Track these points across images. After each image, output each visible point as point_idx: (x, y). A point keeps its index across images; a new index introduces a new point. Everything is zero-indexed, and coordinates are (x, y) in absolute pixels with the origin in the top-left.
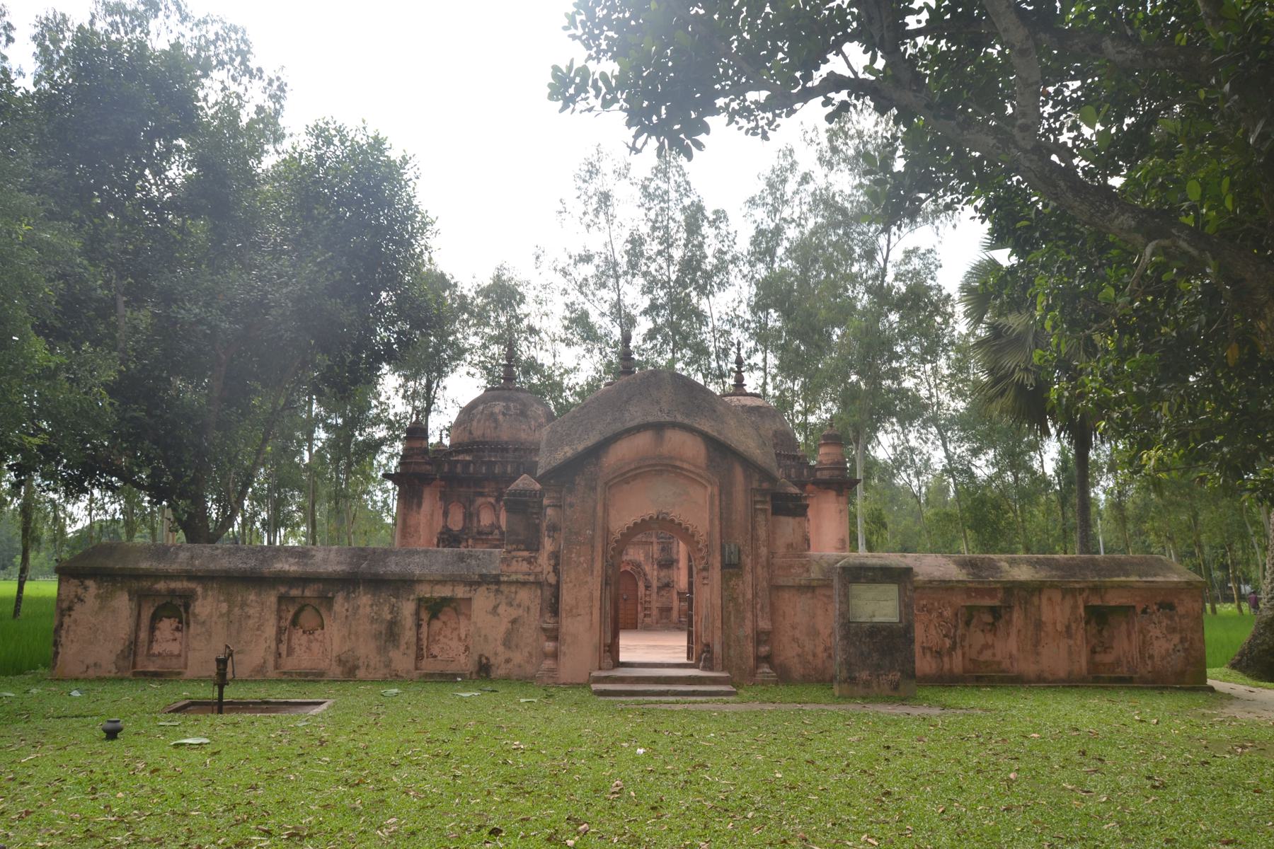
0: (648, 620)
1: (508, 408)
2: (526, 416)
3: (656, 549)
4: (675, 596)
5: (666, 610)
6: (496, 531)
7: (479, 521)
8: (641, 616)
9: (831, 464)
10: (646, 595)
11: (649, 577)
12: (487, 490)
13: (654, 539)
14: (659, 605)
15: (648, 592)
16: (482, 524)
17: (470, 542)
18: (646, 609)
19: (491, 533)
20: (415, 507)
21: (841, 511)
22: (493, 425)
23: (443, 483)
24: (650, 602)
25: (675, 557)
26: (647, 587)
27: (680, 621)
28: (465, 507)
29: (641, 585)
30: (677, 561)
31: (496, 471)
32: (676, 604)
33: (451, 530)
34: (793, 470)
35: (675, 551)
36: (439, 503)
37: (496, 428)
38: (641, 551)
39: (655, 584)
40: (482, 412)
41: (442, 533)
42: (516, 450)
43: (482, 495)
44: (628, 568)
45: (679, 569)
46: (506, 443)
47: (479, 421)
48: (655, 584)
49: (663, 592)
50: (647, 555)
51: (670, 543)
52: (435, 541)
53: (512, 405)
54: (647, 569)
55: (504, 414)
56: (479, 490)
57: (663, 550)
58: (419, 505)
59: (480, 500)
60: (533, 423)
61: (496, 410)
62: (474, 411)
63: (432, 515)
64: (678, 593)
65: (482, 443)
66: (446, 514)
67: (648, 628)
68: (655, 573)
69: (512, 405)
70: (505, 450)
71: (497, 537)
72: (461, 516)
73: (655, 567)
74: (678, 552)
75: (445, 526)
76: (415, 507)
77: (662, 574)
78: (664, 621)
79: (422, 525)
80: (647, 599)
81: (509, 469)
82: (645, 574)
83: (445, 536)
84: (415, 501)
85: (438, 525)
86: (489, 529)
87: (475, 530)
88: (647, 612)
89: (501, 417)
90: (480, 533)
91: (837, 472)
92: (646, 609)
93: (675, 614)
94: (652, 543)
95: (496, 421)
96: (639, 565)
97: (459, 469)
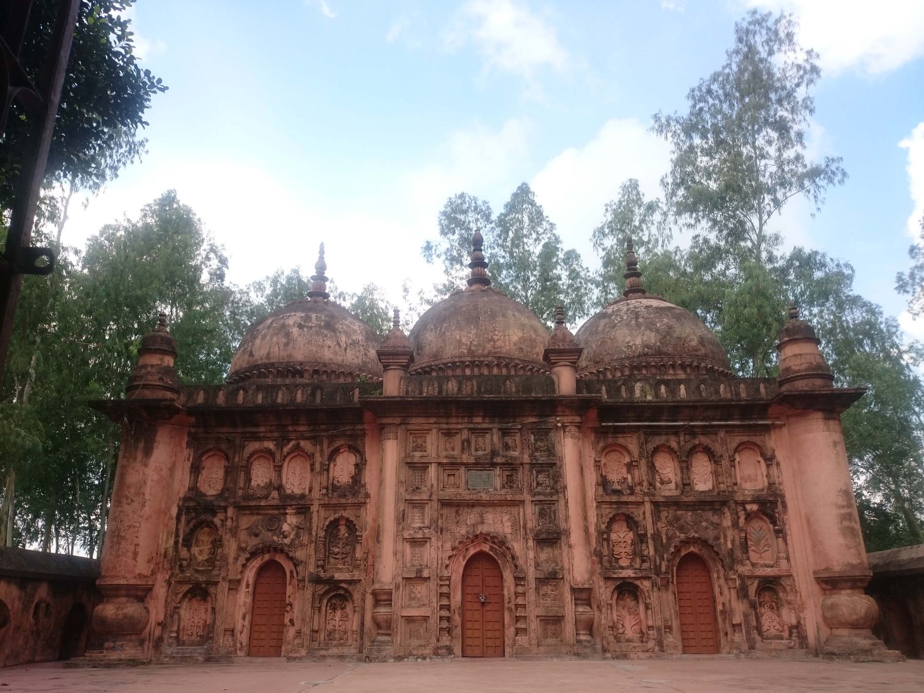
0: (522, 640)
1: (307, 319)
2: (334, 330)
3: (530, 512)
4: (568, 596)
5: (553, 621)
6: (275, 494)
7: (249, 480)
8: (510, 632)
9: (806, 370)
10: (517, 595)
11: (520, 562)
12: (262, 429)
13: (527, 497)
14: (540, 611)
15: (520, 589)
16: (253, 483)
17: (230, 512)
18: (518, 619)
19: (266, 497)
20: (140, 455)
21: (835, 444)
22: (284, 340)
23: (193, 420)
24: (524, 606)
25: (563, 525)
26: (519, 580)
27: (579, 641)
28: (227, 459)
29: (508, 575)
30: (567, 533)
31: (279, 400)
32: (570, 610)
33: (205, 495)
34: (742, 386)
35: (561, 514)
36: (186, 452)
37: (286, 345)
38: (506, 518)
39: (531, 574)
40: (269, 327)
41: (186, 499)
42: (316, 372)
43: (256, 437)
44: (486, 548)
45: (570, 546)
46: (301, 364)
47: (264, 337)
48: (531, 574)
49: (547, 589)
50: (515, 524)
51: (553, 503)
52: (174, 511)
53: (314, 316)
54: (517, 547)
55: (300, 326)
56: (248, 429)
57: (542, 514)
58: (148, 452)
59: (254, 446)
60: (344, 338)
61: (290, 322)
62: (260, 327)
63: (172, 470)
64: (573, 590)
65: (266, 366)
66: (196, 469)
67: (522, 654)
68: (531, 554)
69: (314, 316)
70: (301, 374)
71: (275, 502)
72: (221, 473)
73: (531, 543)
74: (567, 518)
75: (194, 488)
76: (140, 455)
77: (543, 556)
78: (550, 641)
79: (149, 484)
80: (520, 601)
81: (299, 397)
82: (513, 558)
83: (192, 504)
84: (141, 445)
85: (182, 482)
86: (265, 492)
87: (240, 492)
88: (519, 625)
89: (295, 331)
90: (247, 497)
91: (818, 382)
92: (518, 619)
93: (569, 628)
94: (523, 502)
95: (288, 335)
96: (500, 542)
97: (221, 399)
